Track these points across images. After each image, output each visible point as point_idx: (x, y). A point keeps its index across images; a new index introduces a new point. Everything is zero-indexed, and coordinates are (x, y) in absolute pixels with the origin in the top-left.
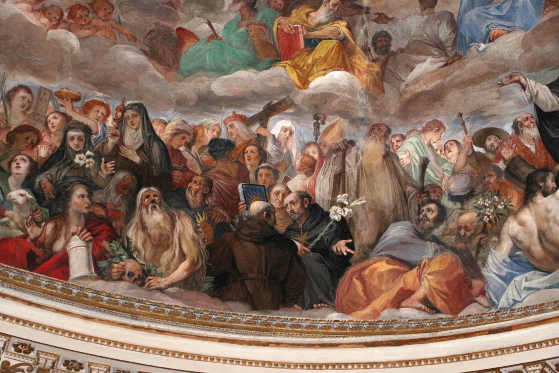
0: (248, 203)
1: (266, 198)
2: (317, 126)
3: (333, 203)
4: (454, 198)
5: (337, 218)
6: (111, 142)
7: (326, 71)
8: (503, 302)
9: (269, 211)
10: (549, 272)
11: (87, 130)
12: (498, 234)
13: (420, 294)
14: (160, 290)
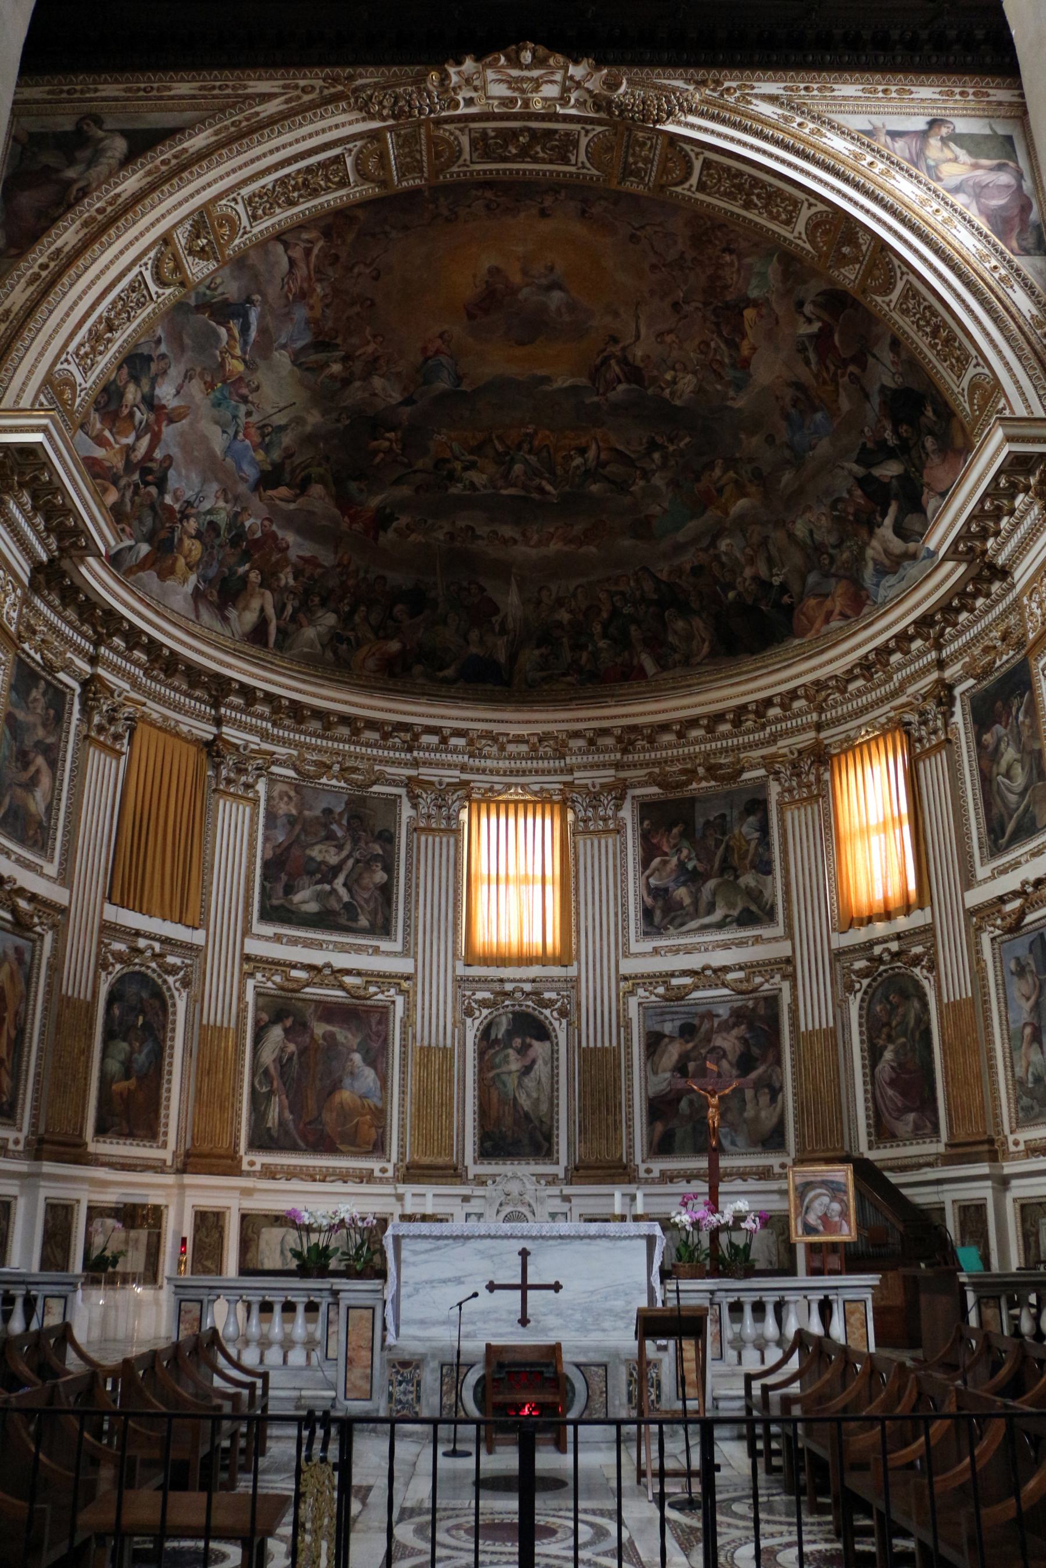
0: (726, 596)
1: (734, 588)
2: (744, 536)
3: (772, 576)
4: (834, 547)
5: (776, 583)
6: (638, 593)
7: (735, 502)
8: (880, 600)
9: (739, 594)
10: (895, 573)
11: (622, 593)
12: (864, 559)
13: (837, 612)
14: (699, 664)
